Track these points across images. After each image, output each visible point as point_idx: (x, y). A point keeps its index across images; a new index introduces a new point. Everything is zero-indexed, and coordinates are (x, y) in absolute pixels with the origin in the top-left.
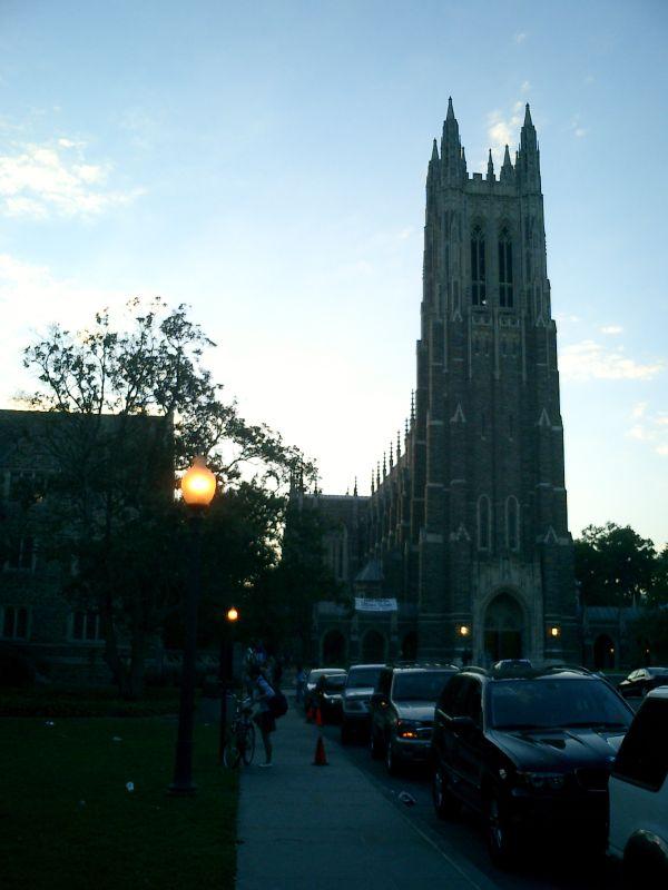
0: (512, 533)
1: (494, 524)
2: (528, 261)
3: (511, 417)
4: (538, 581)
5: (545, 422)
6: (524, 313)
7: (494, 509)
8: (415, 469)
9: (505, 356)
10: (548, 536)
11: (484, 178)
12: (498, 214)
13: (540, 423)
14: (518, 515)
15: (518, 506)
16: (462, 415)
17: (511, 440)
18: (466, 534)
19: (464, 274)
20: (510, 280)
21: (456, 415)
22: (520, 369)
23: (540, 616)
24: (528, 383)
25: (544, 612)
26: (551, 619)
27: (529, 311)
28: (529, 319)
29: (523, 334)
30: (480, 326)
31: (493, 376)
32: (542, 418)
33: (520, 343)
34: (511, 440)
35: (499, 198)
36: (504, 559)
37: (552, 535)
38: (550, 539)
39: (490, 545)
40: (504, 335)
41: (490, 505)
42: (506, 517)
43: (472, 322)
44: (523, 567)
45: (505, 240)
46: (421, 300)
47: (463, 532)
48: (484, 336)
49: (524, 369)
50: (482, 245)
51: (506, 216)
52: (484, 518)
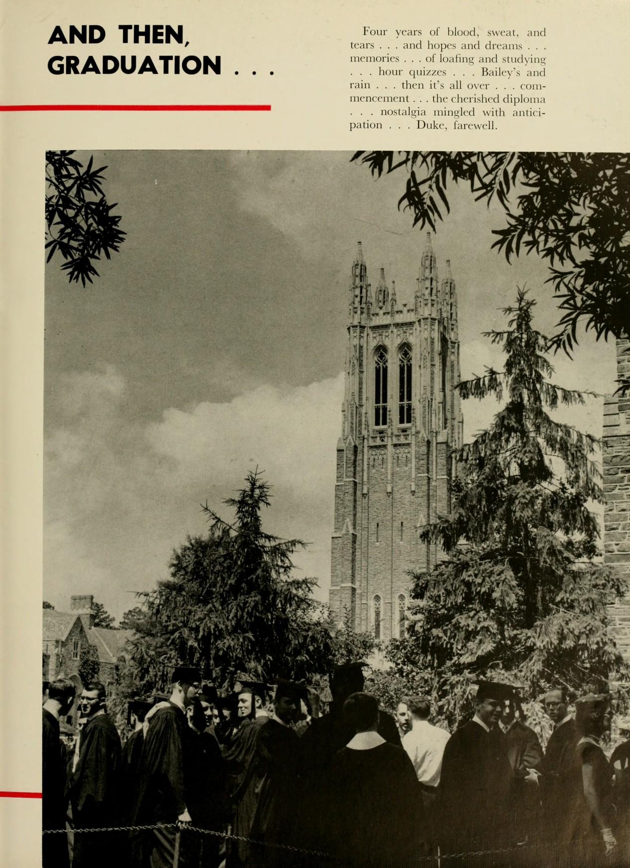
3: (402, 523)
9: (398, 469)
12: (398, 341)
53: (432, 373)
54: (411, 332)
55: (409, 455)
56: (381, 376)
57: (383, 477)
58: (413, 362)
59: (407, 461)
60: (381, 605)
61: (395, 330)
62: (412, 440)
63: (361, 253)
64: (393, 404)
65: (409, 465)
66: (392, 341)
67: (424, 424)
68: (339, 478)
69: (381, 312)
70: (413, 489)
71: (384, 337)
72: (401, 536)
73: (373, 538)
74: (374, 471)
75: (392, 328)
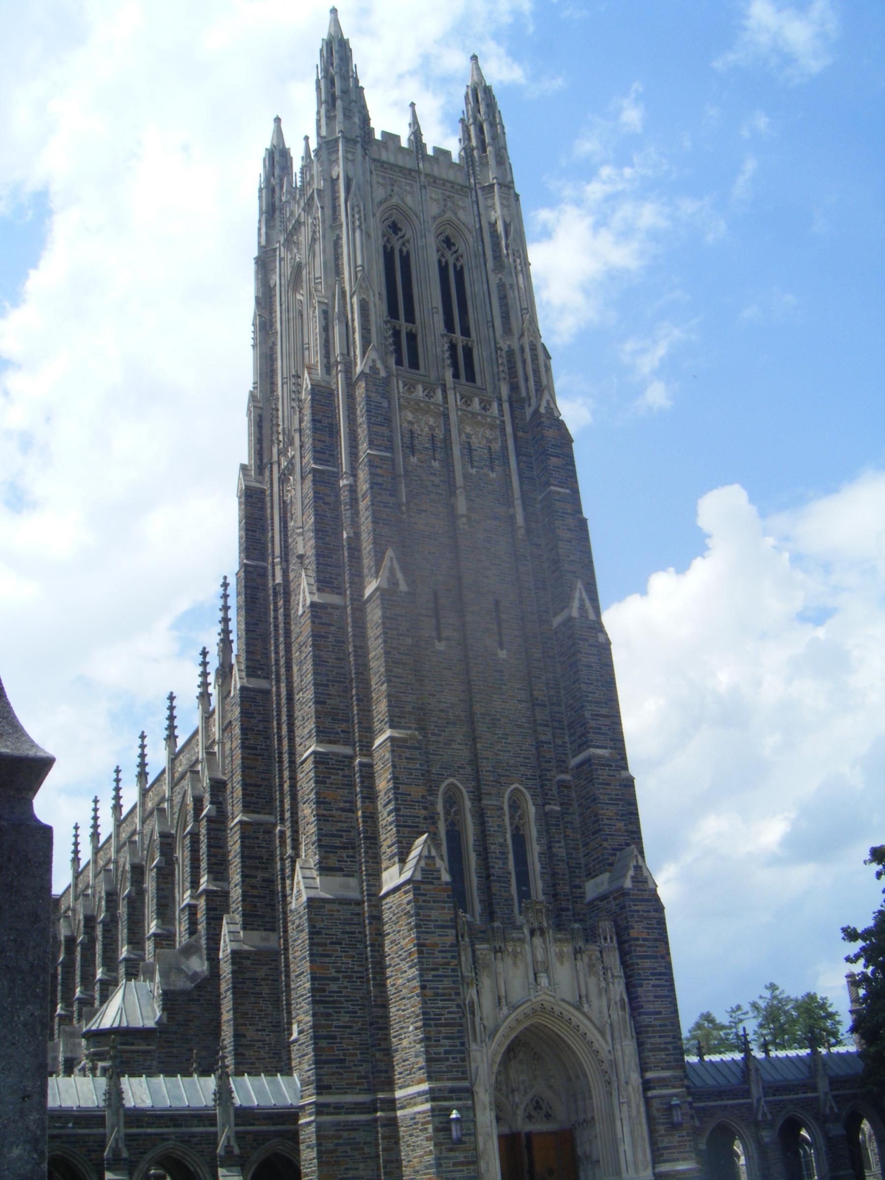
0: (523, 878)
1: (484, 853)
2: (503, 298)
3: (497, 603)
4: (618, 989)
5: (582, 607)
6: (505, 390)
7: (480, 815)
8: (243, 747)
9: (474, 471)
10: (631, 873)
11: (404, 144)
12: (434, 209)
14: (534, 833)
15: (532, 809)
16: (399, 575)
17: (503, 654)
22: (510, 504)
23: (635, 1078)
24: (528, 531)
25: (643, 1068)
26: (663, 1083)
27: (514, 388)
28: (517, 402)
29: (509, 429)
30: (417, 402)
32: (576, 604)
33: (504, 447)
34: (503, 654)
35: (434, 181)
36: (532, 933)
38: (635, 880)
39: (478, 907)
40: (468, 430)
41: (468, 804)
42: (509, 836)
43: (398, 387)
44: (577, 952)
45: (451, 260)
46: (250, 387)
48: (426, 424)
49: (518, 502)
50: (406, 260)
57: (437, 480)
59: (492, 462)
65: (497, 468)
72: (500, 633)
74: (413, 460)
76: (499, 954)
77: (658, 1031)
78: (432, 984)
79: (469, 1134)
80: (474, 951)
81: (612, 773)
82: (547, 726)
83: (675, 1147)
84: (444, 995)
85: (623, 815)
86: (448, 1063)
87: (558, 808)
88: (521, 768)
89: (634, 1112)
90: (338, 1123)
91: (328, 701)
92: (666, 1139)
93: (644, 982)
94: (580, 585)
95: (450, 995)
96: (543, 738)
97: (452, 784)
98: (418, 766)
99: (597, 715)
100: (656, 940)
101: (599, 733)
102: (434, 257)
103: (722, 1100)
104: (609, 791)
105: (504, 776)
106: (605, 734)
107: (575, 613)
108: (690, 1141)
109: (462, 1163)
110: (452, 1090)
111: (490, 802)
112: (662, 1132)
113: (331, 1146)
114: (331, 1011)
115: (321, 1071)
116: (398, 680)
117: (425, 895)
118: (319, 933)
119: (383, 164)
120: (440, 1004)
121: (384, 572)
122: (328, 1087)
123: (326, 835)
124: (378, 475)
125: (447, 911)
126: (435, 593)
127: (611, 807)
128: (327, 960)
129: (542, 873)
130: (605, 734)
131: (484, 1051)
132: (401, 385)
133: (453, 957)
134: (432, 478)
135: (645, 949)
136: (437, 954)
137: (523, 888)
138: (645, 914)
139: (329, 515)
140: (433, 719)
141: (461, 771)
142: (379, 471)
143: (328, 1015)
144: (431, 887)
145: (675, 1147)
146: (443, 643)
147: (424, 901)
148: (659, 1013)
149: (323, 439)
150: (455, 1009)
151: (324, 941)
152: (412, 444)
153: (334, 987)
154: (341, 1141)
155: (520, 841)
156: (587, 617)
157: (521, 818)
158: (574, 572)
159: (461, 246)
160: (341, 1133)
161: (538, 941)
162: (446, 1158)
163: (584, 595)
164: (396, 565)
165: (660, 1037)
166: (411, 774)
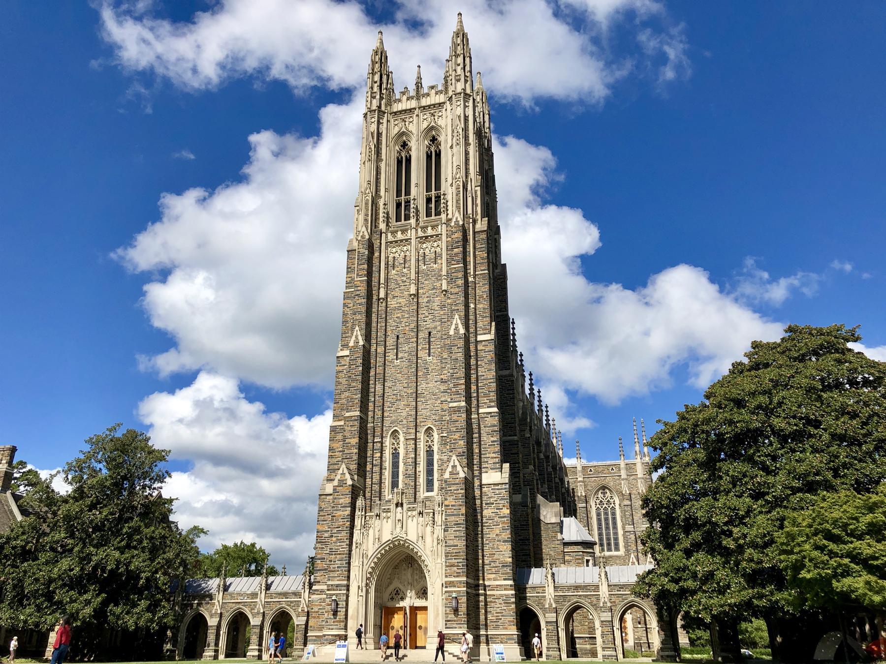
3: (430, 333)
4: (439, 531)
5: (456, 329)
10: (450, 469)
13: (452, 332)
16: (360, 338)
18: (348, 476)
19: (382, 193)
20: (438, 188)
21: (354, 338)
26: (451, 584)
29: (444, 237)
31: (408, 290)
32: (453, 327)
33: (441, 249)
37: (454, 467)
38: (451, 473)
44: (420, 513)
47: (343, 474)
50: (409, 160)
51: (433, 124)
52: (395, 455)
53: (467, 154)
54: (440, 114)
55: (438, 250)
56: (403, 164)
57: (404, 279)
58: (442, 148)
59: (436, 258)
60: (401, 443)
61: (421, 115)
62: (442, 229)
63: (382, 43)
64: (418, 192)
65: (439, 261)
66: (416, 126)
67: (458, 208)
68: (349, 284)
69: (405, 98)
70: (444, 287)
71: (407, 123)
73: (391, 356)
74: (394, 272)
75: (416, 112)
76: (378, 517)
77: (455, 556)
78: (336, 535)
79: (343, 608)
80: (365, 517)
81: (460, 415)
82: (446, 392)
83: (455, 621)
84: (341, 539)
85: (463, 437)
86: (338, 573)
87: (446, 435)
88: (433, 416)
89: (436, 600)
90: (321, 599)
91: (340, 402)
92: (450, 616)
93: (449, 529)
94: (457, 316)
95: (344, 539)
96: (443, 399)
97: (396, 430)
98: (356, 429)
99: (457, 385)
100: (460, 505)
101: (457, 394)
102: (423, 150)
103: (577, 592)
104: (457, 425)
105: (423, 422)
106: (461, 394)
107: (452, 332)
108: (465, 618)
109: (337, 621)
110: (337, 586)
111: (410, 437)
112: (447, 612)
113: (317, 610)
114: (324, 546)
115: (316, 575)
116: (353, 389)
117: (338, 492)
118: (322, 510)
119: (395, 113)
120: (338, 544)
121: (354, 338)
122: (319, 582)
123: (331, 464)
124: (358, 290)
125: (348, 499)
126: (398, 336)
127: (457, 434)
128: (325, 522)
129: (438, 470)
130: (461, 394)
131: (361, 566)
132: (389, 234)
133: (347, 521)
134: (402, 278)
135: (453, 511)
136: (340, 520)
137: (430, 478)
138: (455, 492)
139: (349, 313)
140: (389, 400)
141: (401, 423)
142: (359, 288)
143: (323, 548)
144: (342, 488)
145: (455, 621)
146: (398, 361)
147: (337, 495)
148: (457, 546)
149: (351, 276)
150: (345, 546)
151: (324, 514)
152: (394, 264)
153: (326, 535)
154: (321, 607)
155: (430, 453)
156: (458, 333)
157: (432, 441)
158: (458, 310)
159: (441, 139)
160: (322, 603)
161: (399, 509)
162: (330, 619)
163: (459, 321)
164: (359, 333)
165: (455, 559)
166: (352, 433)
